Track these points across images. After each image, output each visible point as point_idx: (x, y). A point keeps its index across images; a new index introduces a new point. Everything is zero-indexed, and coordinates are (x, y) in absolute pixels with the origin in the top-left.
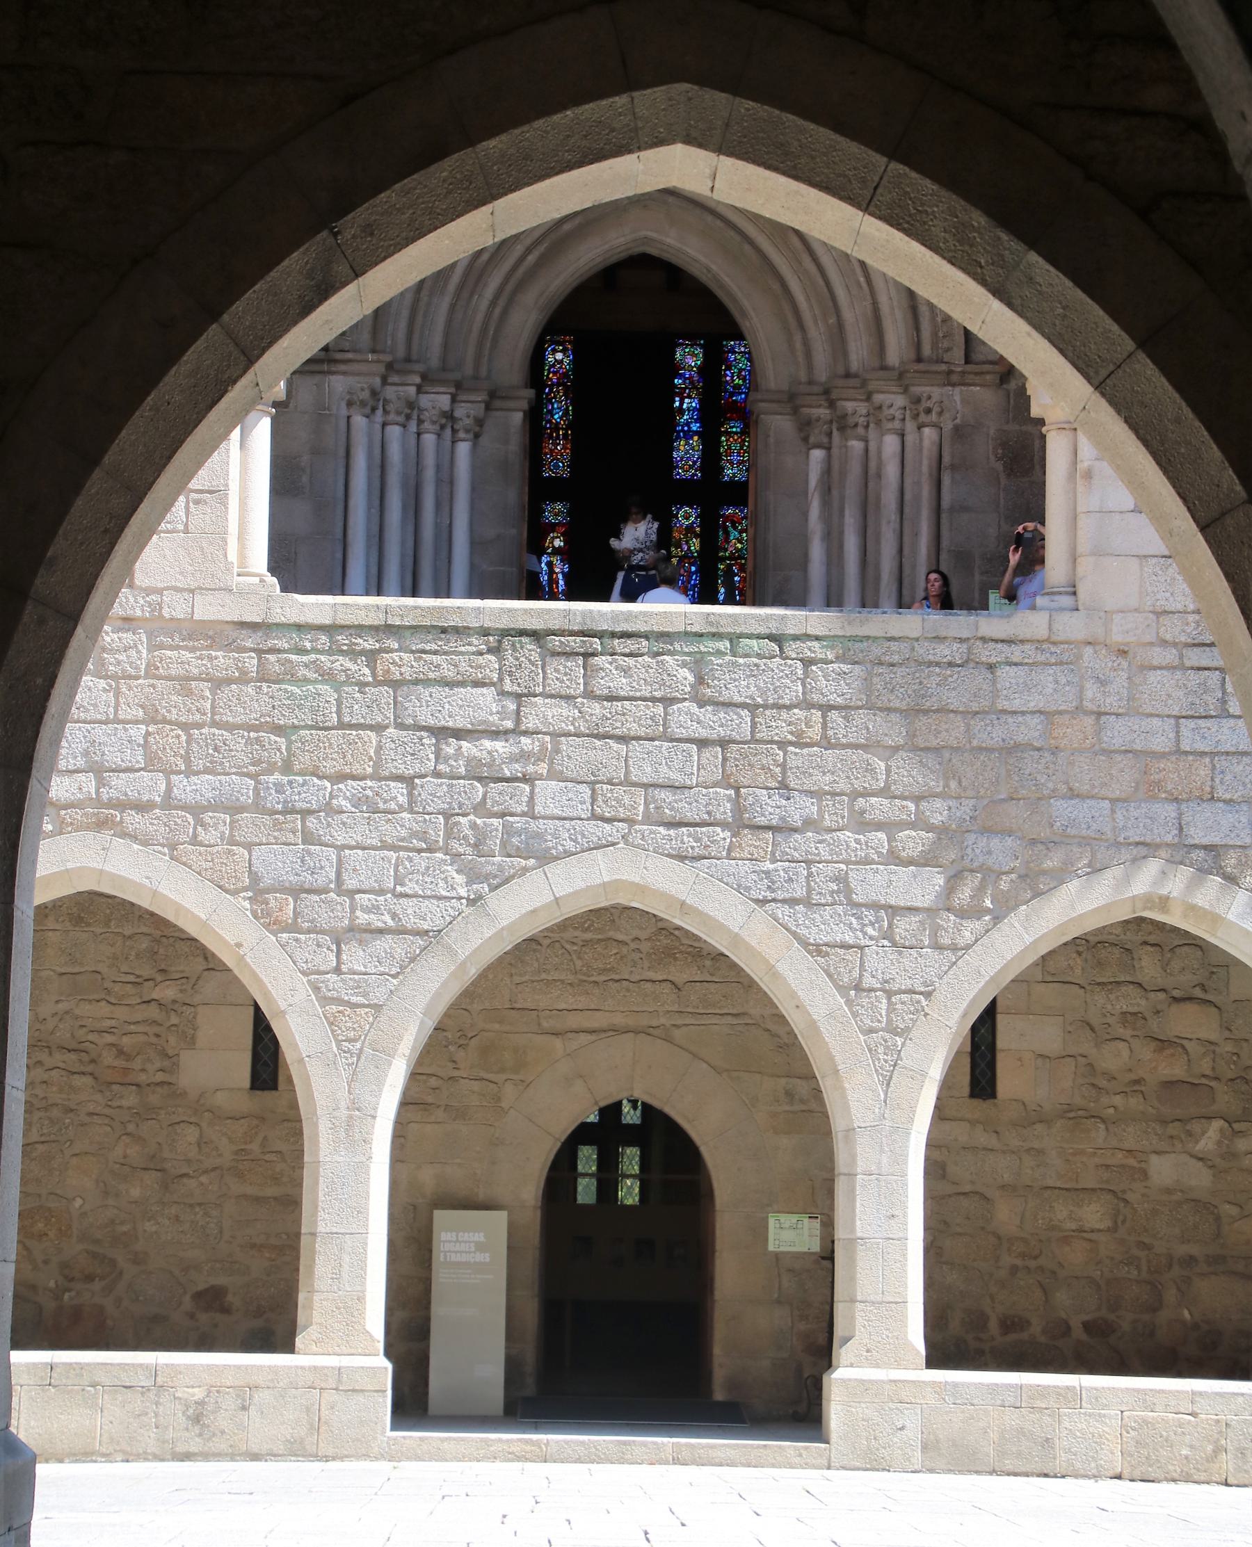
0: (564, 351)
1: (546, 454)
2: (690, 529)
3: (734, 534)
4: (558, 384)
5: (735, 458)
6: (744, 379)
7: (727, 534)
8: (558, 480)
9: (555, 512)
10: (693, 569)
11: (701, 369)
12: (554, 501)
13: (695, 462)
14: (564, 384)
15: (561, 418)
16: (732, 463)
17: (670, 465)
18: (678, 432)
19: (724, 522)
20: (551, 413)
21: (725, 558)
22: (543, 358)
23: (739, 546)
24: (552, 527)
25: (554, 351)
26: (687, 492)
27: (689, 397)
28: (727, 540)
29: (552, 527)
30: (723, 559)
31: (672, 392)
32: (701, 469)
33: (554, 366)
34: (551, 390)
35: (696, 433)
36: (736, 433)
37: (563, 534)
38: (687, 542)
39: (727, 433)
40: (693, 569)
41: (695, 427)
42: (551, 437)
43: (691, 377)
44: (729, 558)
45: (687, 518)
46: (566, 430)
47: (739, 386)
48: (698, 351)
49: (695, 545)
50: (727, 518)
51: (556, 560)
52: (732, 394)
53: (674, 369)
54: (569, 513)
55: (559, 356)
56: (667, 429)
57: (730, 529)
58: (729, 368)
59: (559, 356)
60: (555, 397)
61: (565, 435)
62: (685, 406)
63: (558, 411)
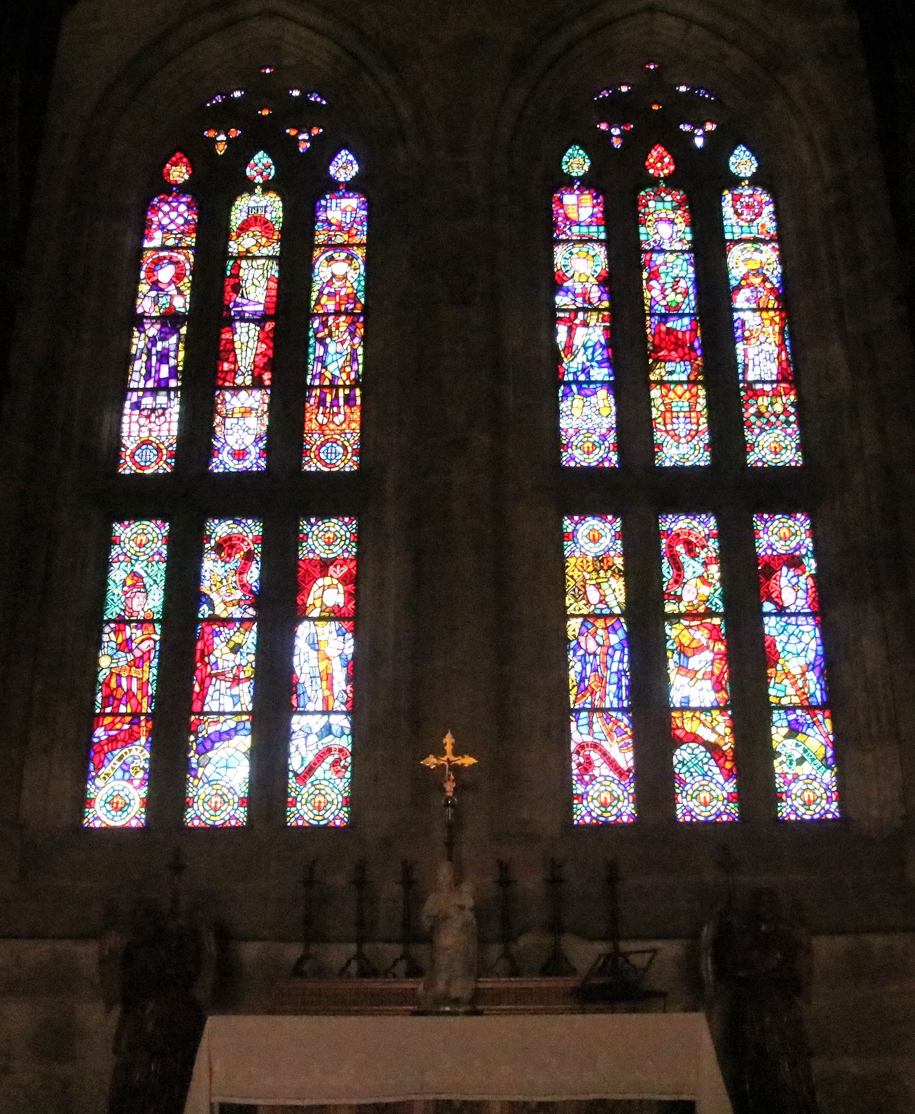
0: (350, 258)
1: (312, 432)
2: (601, 563)
3: (692, 567)
4: (337, 313)
5: (682, 427)
6: (686, 294)
7: (678, 567)
8: (336, 479)
9: (327, 538)
10: (614, 639)
11: (604, 282)
12: (324, 515)
13: (604, 437)
14: (347, 313)
15: (342, 370)
16: (676, 437)
17: (554, 441)
18: (568, 384)
19: (670, 547)
20: (321, 360)
21: (679, 616)
22: (309, 268)
23: (705, 591)
24: (324, 566)
25: (331, 259)
26: (590, 492)
27: (585, 324)
28: (679, 580)
29: (324, 566)
30: (677, 617)
31: (551, 317)
32: (619, 447)
33: (329, 283)
34: (324, 324)
35: (603, 383)
36: (680, 383)
37: (343, 580)
38: (598, 586)
39: (662, 383)
40: (614, 639)
41: (601, 374)
42: (321, 402)
43: (585, 295)
44: (691, 615)
45: (594, 541)
46: (352, 388)
47: (678, 307)
48: (600, 251)
49: (615, 593)
50: (675, 538)
51: (328, 632)
52: (664, 318)
53: (555, 284)
54: (359, 539)
55: (340, 268)
56: (546, 381)
57: (685, 559)
58: (654, 275)
59: (340, 268)
60: (330, 335)
61: (349, 400)
62: (578, 340)
63: (337, 355)
